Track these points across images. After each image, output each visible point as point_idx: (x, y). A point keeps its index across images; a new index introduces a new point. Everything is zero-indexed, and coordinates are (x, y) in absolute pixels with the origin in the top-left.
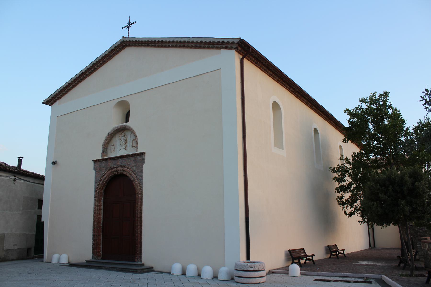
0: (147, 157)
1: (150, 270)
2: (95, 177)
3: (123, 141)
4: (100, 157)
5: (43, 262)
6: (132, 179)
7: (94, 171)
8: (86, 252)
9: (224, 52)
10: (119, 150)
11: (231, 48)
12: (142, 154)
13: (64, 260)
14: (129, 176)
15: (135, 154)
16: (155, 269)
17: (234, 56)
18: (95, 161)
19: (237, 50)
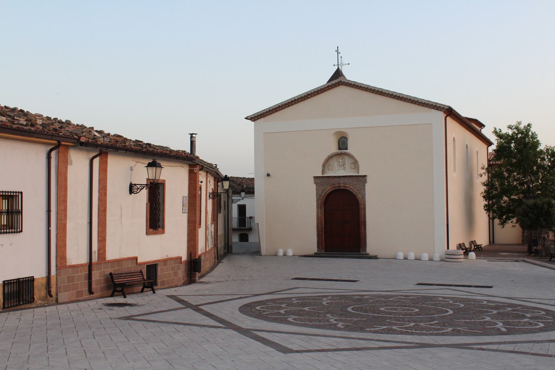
0: (368, 179)
1: (375, 257)
2: (317, 190)
3: (341, 163)
4: (320, 175)
5: (261, 255)
6: (355, 194)
7: (315, 185)
8: (313, 248)
9: (434, 111)
10: (338, 170)
11: (441, 110)
12: (365, 176)
13: (290, 253)
14: (352, 191)
15: (356, 176)
16: (378, 257)
17: (442, 115)
18: (315, 178)
19: (445, 112)
